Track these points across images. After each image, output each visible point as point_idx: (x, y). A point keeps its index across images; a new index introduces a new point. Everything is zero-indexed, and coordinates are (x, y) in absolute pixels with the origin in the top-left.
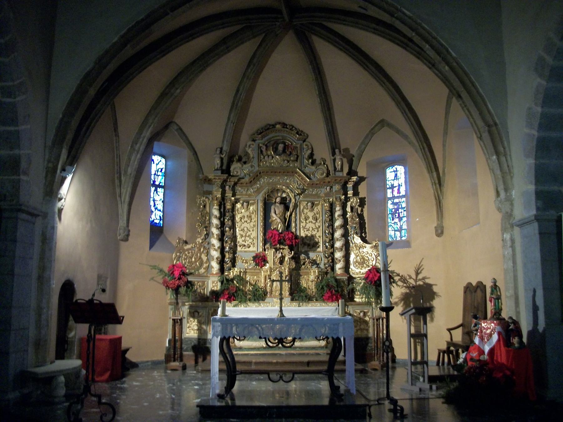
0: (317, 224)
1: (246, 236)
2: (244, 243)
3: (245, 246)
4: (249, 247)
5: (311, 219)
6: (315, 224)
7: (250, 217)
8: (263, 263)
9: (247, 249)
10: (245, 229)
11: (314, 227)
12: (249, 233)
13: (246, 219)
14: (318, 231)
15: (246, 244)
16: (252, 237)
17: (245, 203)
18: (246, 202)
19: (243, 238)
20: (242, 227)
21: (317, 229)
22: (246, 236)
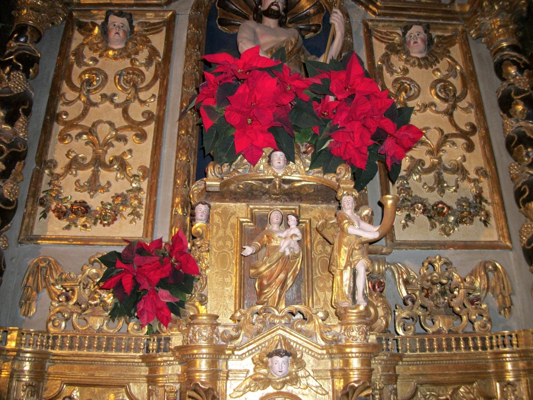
0: (464, 117)
1: (98, 162)
2: (84, 196)
3: (83, 209)
4: (108, 216)
5: (429, 95)
6: (449, 113)
7: (132, 80)
8: (165, 296)
9: (98, 230)
10: (104, 131)
11: (449, 129)
12: (118, 149)
13: (109, 88)
14: (470, 147)
15: (95, 203)
16: (133, 170)
17: (114, 19)
18: (120, 14)
19: (84, 175)
20: (87, 122)
21: (464, 135)
22: (98, 162)
